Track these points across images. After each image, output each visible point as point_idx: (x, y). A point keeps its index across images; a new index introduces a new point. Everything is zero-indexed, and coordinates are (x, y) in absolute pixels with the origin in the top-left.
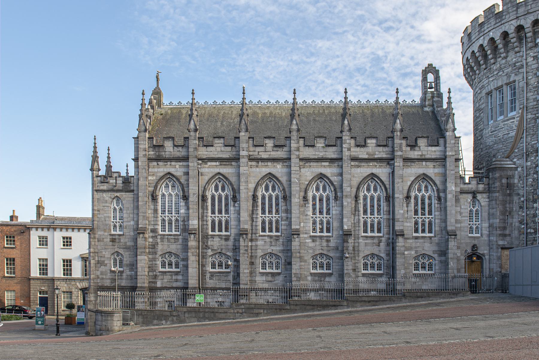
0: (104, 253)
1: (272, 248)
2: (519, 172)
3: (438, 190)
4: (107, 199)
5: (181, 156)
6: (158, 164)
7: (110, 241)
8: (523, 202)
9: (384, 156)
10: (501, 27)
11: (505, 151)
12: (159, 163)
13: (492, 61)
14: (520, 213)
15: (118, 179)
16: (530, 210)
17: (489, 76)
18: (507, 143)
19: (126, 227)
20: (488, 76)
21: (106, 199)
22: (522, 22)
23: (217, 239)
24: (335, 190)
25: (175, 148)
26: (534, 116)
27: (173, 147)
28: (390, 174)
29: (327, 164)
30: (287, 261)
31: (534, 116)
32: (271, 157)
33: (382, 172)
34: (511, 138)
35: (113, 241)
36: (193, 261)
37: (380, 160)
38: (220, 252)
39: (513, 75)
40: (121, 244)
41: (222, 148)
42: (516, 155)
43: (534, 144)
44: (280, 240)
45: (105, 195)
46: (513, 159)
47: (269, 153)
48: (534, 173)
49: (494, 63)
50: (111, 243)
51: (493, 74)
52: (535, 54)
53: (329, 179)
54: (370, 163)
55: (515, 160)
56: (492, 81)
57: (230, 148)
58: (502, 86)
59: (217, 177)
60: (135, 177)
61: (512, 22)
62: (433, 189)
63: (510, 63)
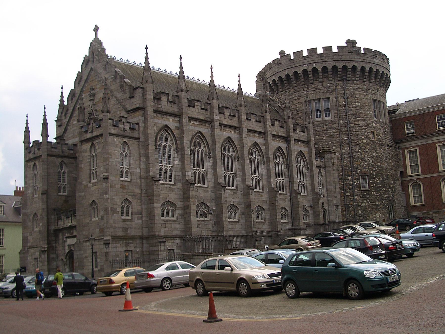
0: (115, 200)
1: (233, 200)
2: (337, 156)
3: (307, 162)
4: (117, 143)
5: (173, 112)
6: (157, 116)
7: (121, 188)
8: (342, 175)
9: (283, 135)
10: (322, 63)
11: (325, 141)
12: (158, 114)
13: (312, 81)
14: (340, 182)
15: (125, 124)
16: (347, 180)
17: (308, 91)
18: (327, 136)
19: (133, 173)
20: (307, 90)
21: (116, 143)
22: (336, 64)
23: (200, 190)
24: (263, 155)
25: (169, 103)
26: (344, 122)
27: (168, 102)
28: (287, 148)
29: (257, 135)
30: (242, 212)
31: (344, 122)
32: (228, 124)
33: (283, 145)
34: (329, 134)
35: (123, 187)
36: (194, 210)
37: (281, 137)
38: (202, 203)
39: (328, 94)
40: (130, 191)
41: (200, 110)
42: (335, 144)
43: (346, 139)
44: (238, 194)
45: (115, 139)
46: (333, 147)
47: (226, 120)
48: (347, 158)
49: (312, 83)
50: (121, 189)
51: (310, 90)
52: (342, 85)
53: (259, 147)
54: (277, 138)
55: (334, 148)
56: (311, 94)
57: (204, 111)
58: (319, 99)
59: (198, 135)
60: (140, 125)
61: (330, 62)
62: (304, 162)
63: (325, 86)
